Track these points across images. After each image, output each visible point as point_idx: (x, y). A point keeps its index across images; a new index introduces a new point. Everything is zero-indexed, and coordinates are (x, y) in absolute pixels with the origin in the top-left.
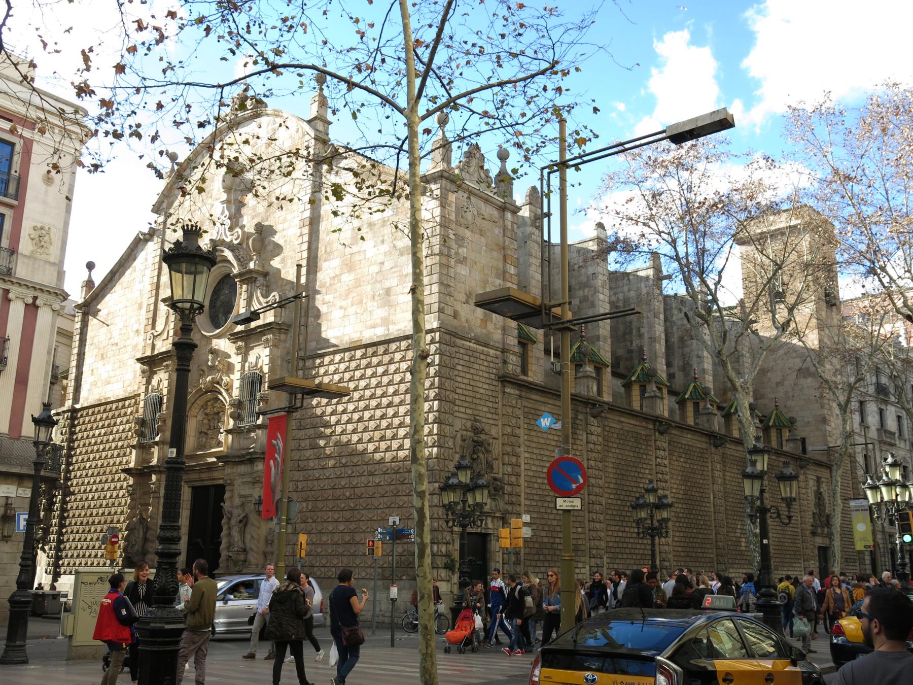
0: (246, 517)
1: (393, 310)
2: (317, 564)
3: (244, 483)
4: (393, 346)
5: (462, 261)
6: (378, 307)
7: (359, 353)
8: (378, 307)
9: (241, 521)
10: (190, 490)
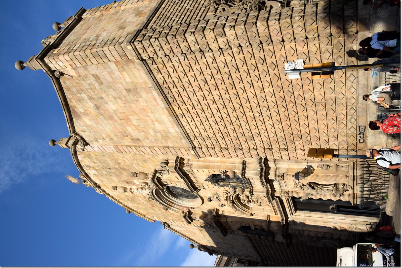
0: (310, 184)
1: (138, 86)
2: (345, 131)
3: (286, 185)
4: (161, 82)
5: (98, 36)
6: (141, 97)
7: (176, 108)
8: (141, 97)
9: (313, 188)
10: (298, 211)
